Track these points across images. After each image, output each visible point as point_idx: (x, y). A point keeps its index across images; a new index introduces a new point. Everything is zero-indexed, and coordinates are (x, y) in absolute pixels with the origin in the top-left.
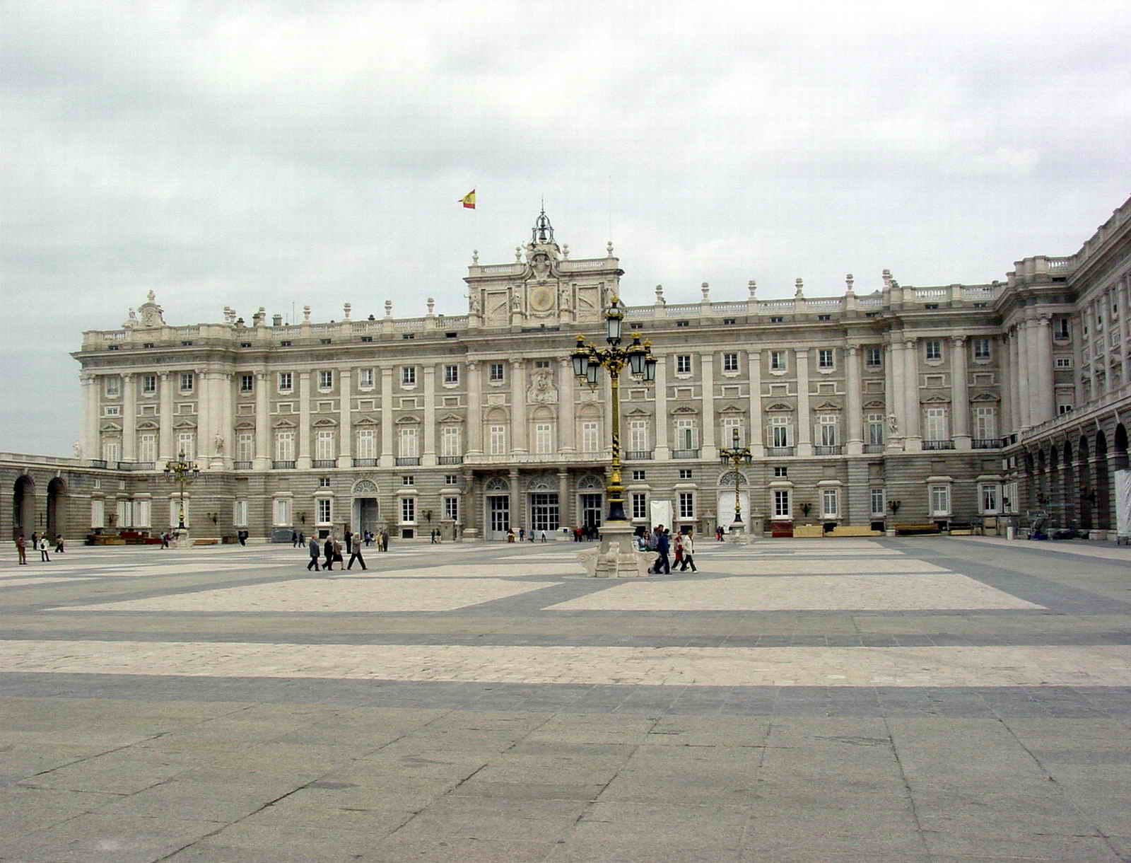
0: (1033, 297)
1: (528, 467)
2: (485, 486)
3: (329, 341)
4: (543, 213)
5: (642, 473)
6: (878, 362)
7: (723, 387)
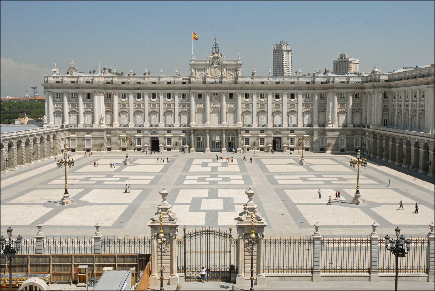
0: (378, 87)
1: (213, 129)
2: (196, 135)
3: (140, 83)
4: (216, 42)
5: (248, 131)
6: (324, 98)
7: (275, 104)
